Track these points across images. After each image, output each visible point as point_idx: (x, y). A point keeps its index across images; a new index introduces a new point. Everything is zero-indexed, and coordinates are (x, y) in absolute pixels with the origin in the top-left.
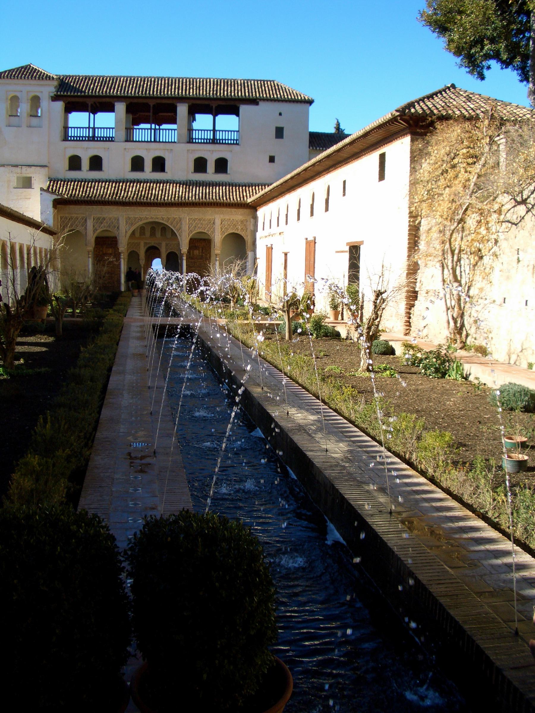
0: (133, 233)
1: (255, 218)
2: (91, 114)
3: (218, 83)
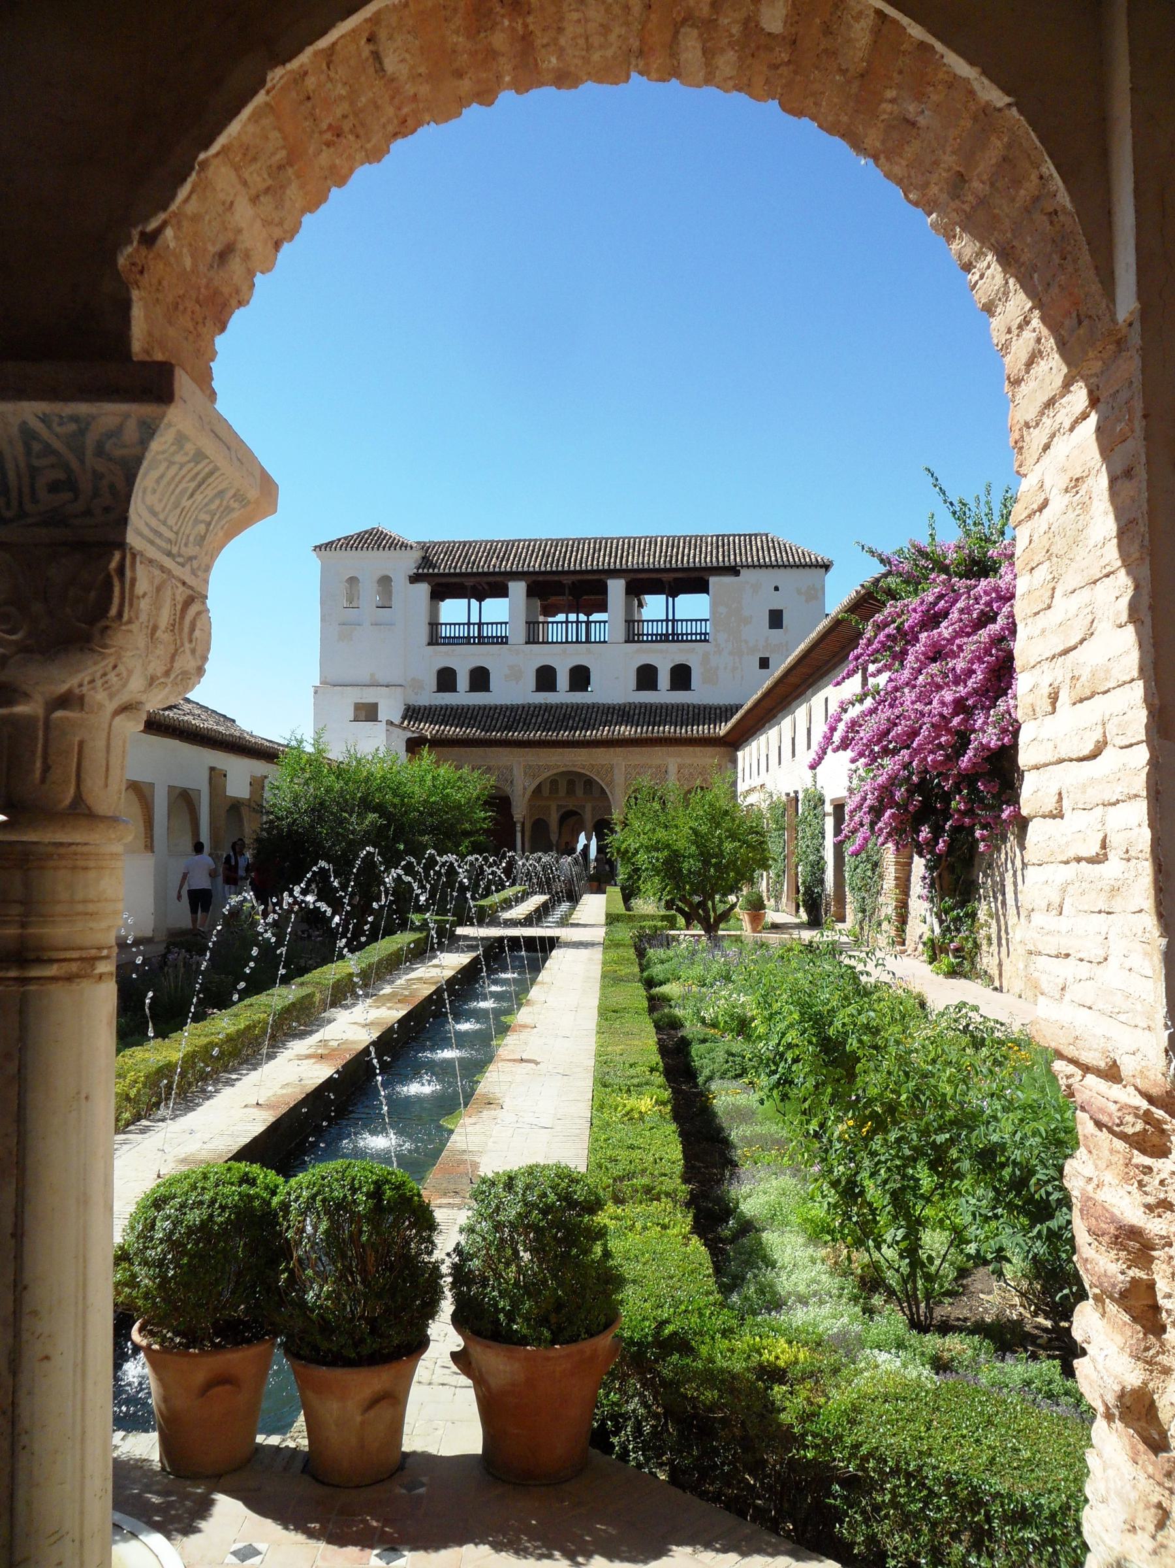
0: (538, 790)
1: (734, 761)
2: (473, 601)
3: (673, 542)
